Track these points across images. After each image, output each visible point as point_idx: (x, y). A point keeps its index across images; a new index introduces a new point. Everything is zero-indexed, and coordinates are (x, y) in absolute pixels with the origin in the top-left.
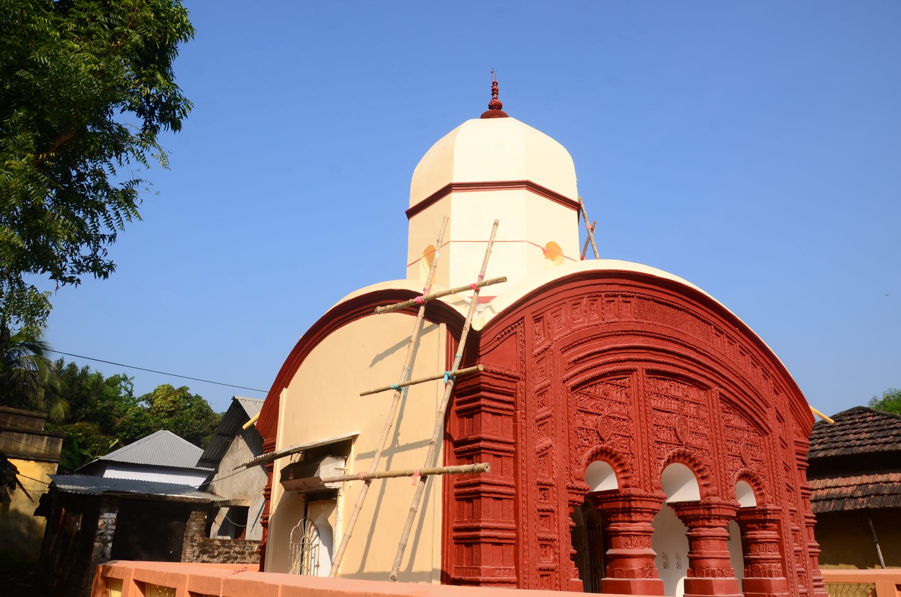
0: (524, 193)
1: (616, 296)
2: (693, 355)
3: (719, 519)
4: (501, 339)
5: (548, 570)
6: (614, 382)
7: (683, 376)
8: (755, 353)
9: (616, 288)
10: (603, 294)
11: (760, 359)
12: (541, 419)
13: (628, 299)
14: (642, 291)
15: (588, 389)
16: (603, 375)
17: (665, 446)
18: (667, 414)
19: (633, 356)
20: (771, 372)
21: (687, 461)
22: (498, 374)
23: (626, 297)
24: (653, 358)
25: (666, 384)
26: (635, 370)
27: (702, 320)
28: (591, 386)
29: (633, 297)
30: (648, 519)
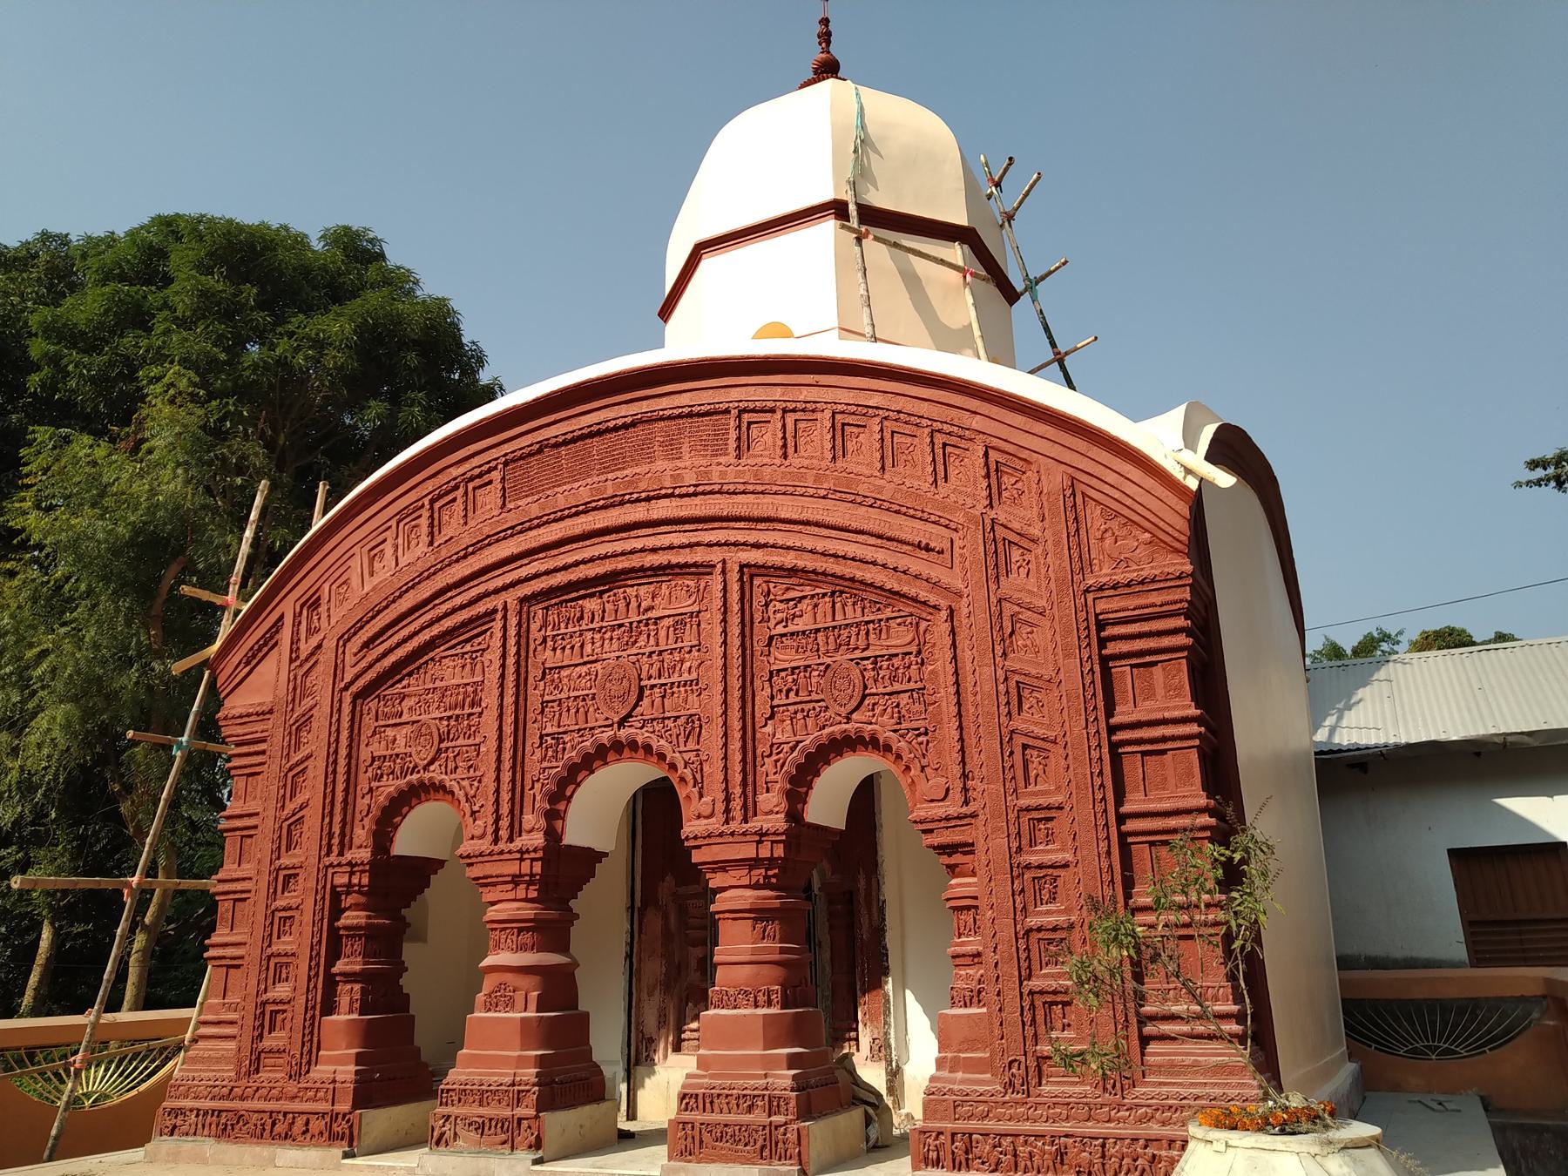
0: (708, 264)
1: (456, 488)
2: (662, 509)
3: (724, 870)
4: (254, 659)
5: (281, 1002)
6: (458, 650)
7: (625, 572)
8: (899, 404)
9: (455, 472)
10: (426, 501)
11: (924, 409)
12: (297, 764)
13: (486, 478)
14: (507, 448)
15: (405, 683)
16: (430, 645)
17: (567, 738)
18: (584, 669)
19: (492, 585)
20: (977, 423)
21: (626, 751)
22: (241, 717)
23: (480, 476)
24: (543, 568)
25: (592, 605)
26: (495, 611)
27: (699, 415)
28: (410, 674)
29: (495, 468)
30: (511, 895)
